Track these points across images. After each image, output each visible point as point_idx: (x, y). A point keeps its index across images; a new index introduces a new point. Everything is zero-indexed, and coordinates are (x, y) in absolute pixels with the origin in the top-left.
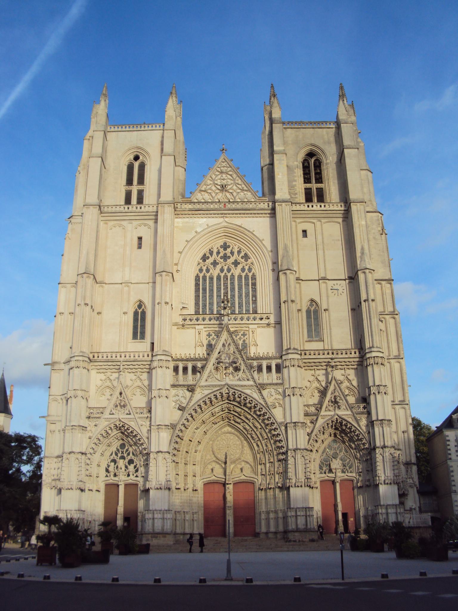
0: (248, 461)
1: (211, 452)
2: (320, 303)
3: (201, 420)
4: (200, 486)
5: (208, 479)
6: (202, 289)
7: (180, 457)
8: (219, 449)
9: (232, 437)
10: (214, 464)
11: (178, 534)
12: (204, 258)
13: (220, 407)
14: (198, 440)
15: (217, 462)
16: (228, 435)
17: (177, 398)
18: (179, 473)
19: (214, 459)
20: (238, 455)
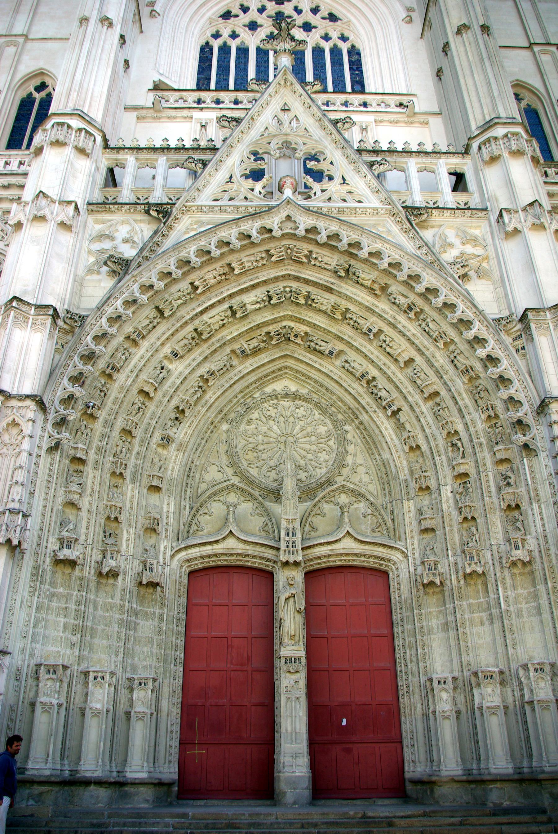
0: (363, 491)
1: (224, 458)
2: (542, 90)
3: (190, 328)
4: (172, 568)
5: (207, 550)
6: (219, 67)
7: (96, 443)
8: (254, 450)
9: (301, 412)
10: (232, 498)
11: (87, 783)
12: (227, 15)
13: (260, 293)
14: (175, 402)
16: (286, 403)
17: (107, 245)
18: (84, 503)
19: (235, 480)
20: (324, 471)
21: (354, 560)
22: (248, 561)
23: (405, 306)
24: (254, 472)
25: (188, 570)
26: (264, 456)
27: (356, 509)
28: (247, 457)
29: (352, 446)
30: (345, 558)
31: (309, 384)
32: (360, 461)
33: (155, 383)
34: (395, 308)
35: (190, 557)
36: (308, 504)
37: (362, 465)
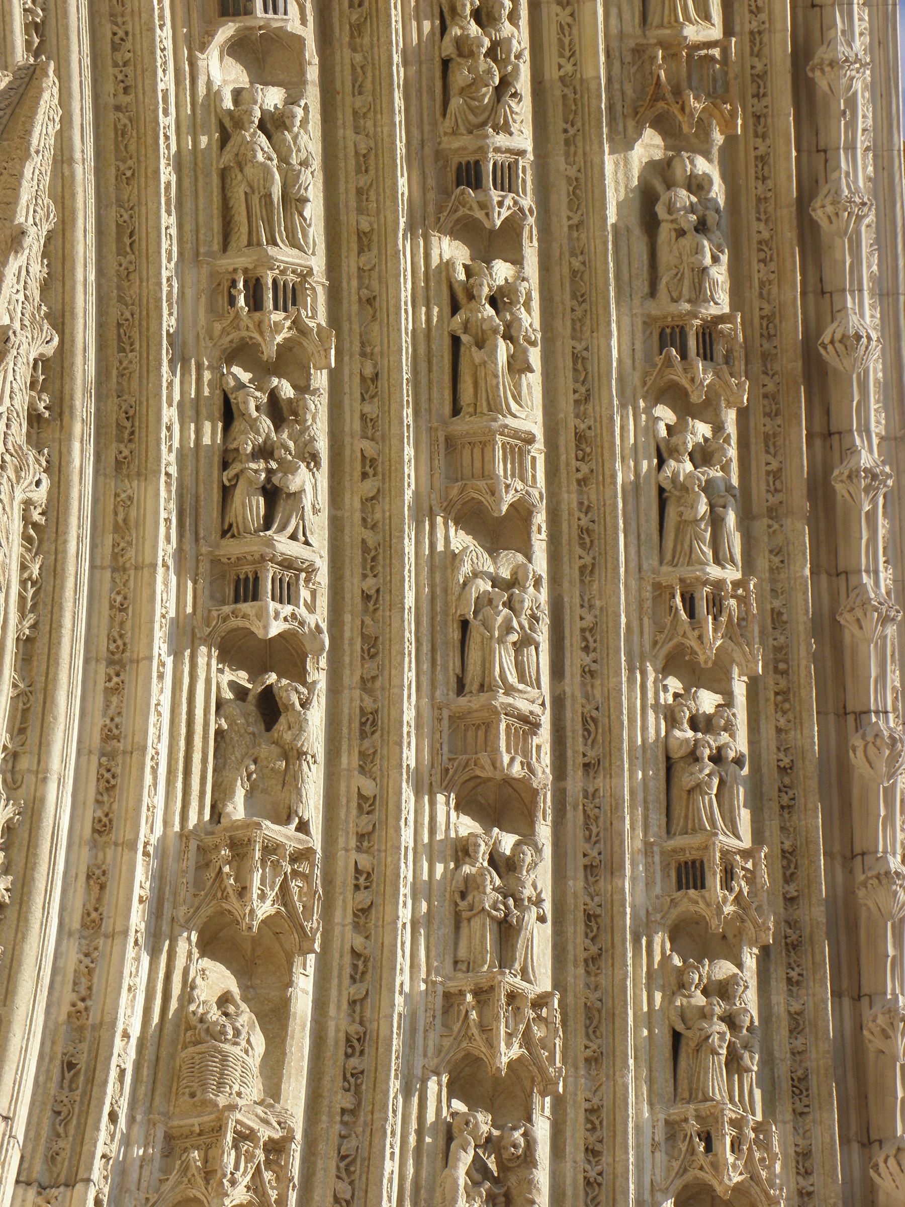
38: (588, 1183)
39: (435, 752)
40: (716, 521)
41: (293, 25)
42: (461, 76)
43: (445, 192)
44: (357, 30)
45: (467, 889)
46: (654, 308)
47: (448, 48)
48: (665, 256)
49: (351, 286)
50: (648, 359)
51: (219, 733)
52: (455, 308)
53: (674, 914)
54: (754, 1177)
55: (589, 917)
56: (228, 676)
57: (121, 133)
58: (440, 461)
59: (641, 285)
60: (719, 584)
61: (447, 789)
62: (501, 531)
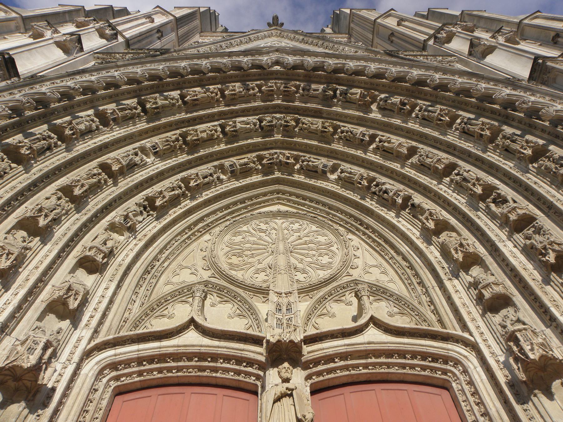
1: (200, 263)
9: (296, 226)
15: (220, 290)
16: (279, 221)
21: (389, 365)
22: (215, 370)
23: (398, 102)
24: (238, 275)
25: (113, 384)
26: (251, 260)
27: (377, 308)
28: (230, 261)
29: (360, 250)
30: (373, 360)
31: (304, 205)
32: (372, 262)
33: (122, 160)
34: (387, 112)
35: (119, 358)
36: (308, 303)
37: (376, 266)
38: (514, 182)
39: (437, 178)
40: (429, 111)
41: (331, 163)
42: (348, 138)
43: (363, 145)
44: (336, 153)
45: (457, 183)
46: (396, 112)
47: (344, 139)
48: (389, 108)
49: (368, 166)
50: (403, 115)
51: (412, 216)
52: (379, 149)
53: (486, 142)
54: (532, 147)
55: (476, 160)
56: (407, 210)
57: (334, 195)
58: (399, 159)
59: (392, 113)
60: (439, 114)
61: (442, 179)
62: (412, 151)
